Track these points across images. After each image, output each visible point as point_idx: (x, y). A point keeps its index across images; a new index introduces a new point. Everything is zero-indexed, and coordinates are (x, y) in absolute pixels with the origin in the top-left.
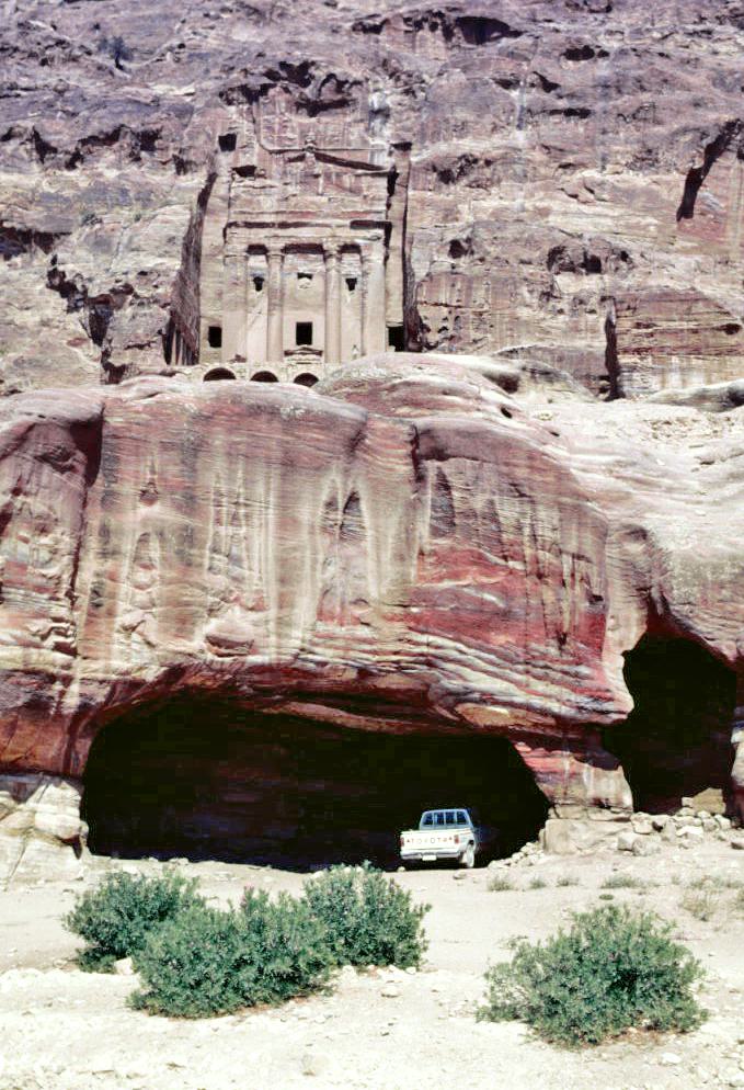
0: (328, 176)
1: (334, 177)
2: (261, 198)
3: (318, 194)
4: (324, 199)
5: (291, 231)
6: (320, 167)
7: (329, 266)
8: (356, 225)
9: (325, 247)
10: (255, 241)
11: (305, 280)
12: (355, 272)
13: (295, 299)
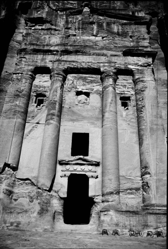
0: (100, 26)
1: (105, 25)
2: (47, 37)
3: (94, 35)
4: (99, 38)
5: (72, 58)
6: (95, 18)
7: (105, 84)
8: (128, 52)
9: (102, 69)
10: (40, 64)
11: (83, 97)
12: (129, 92)
13: (73, 112)
